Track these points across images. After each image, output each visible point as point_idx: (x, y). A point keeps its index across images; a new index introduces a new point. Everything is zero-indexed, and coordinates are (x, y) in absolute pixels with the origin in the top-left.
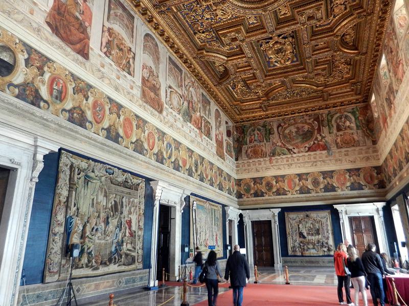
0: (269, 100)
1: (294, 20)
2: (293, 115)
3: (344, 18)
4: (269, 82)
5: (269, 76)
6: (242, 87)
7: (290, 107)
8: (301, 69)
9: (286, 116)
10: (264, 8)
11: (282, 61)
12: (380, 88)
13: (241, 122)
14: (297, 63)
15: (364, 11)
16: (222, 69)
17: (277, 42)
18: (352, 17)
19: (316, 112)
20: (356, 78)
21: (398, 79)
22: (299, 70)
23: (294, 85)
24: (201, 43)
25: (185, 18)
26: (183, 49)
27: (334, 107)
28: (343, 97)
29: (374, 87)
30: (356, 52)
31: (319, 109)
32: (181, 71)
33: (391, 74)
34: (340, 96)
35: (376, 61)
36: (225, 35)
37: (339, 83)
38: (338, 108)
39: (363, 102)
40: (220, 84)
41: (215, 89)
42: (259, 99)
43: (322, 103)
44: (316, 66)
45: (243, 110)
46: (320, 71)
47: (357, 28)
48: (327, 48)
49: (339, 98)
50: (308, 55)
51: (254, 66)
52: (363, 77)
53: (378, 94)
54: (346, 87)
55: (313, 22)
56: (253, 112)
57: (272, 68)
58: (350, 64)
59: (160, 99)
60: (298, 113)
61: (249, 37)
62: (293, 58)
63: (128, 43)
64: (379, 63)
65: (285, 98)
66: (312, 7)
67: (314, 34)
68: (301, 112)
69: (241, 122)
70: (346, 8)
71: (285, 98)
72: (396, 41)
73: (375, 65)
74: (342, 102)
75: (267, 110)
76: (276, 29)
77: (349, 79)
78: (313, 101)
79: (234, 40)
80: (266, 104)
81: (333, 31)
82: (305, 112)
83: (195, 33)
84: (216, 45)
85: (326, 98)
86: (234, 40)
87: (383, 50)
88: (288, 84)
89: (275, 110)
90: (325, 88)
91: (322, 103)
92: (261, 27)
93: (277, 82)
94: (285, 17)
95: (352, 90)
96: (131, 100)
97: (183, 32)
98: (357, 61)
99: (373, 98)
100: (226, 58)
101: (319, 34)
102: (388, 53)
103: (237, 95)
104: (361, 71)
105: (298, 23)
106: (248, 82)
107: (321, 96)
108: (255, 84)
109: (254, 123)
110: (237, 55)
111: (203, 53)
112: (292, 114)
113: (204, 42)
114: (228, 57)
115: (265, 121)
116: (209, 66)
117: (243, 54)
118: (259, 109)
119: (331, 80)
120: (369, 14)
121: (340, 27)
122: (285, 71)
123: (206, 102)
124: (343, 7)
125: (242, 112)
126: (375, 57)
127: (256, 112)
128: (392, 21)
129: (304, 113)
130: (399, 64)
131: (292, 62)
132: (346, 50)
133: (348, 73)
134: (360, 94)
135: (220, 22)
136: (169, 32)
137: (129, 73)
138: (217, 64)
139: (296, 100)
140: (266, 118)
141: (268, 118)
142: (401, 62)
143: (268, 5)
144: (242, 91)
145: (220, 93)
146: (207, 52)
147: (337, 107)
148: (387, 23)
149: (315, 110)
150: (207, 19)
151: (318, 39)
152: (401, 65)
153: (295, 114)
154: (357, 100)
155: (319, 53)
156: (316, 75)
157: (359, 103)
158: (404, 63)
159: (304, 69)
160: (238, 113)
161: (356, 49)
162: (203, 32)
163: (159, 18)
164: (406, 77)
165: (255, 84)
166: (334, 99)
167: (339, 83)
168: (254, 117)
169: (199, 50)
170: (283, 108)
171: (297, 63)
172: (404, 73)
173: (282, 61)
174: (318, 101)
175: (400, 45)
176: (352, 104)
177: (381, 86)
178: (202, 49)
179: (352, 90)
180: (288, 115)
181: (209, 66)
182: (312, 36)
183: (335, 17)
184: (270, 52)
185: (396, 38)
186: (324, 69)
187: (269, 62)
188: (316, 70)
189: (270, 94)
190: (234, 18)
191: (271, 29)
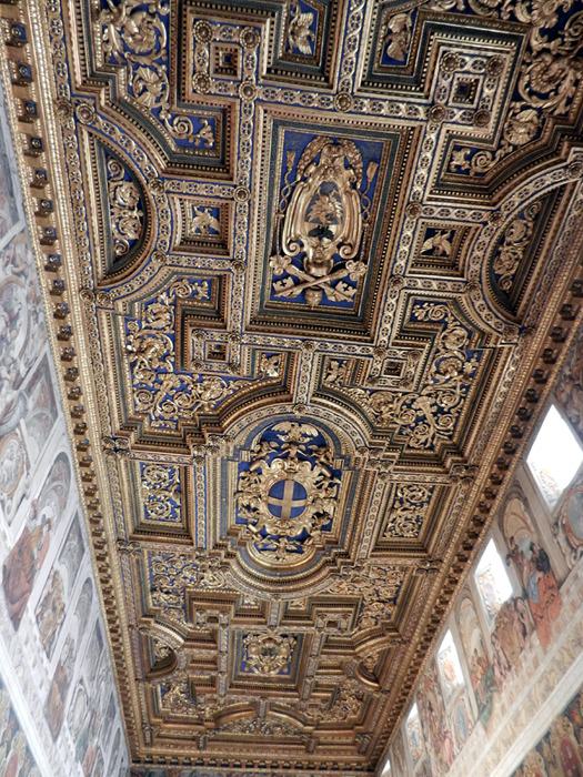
0: (218, 729)
1: (309, 619)
2: (249, 770)
3: (373, 635)
4: (233, 697)
5: (237, 686)
6: (182, 693)
7: (248, 751)
8: (291, 690)
9: (236, 769)
10: (276, 594)
11: (266, 668)
12: (404, 758)
13: (146, 762)
14: (287, 676)
15: (400, 636)
16: (164, 653)
17: (270, 639)
18: (384, 639)
19: (290, 771)
20: (365, 725)
21: (441, 761)
22: (287, 690)
23: (270, 712)
24: (154, 605)
25: (150, 565)
26: (121, 611)
27: (321, 769)
28: (338, 751)
29: (391, 751)
30: (376, 685)
31: (297, 768)
32: (101, 645)
33: (428, 745)
34: (334, 750)
35: (401, 709)
36: (201, 610)
37: (338, 727)
38: (328, 772)
39: (369, 770)
40: (147, 679)
41: (132, 686)
42: (200, 721)
43: (302, 756)
44: (314, 691)
45: (159, 736)
46: (318, 702)
47: (385, 655)
48: (338, 668)
49: (330, 751)
50: (310, 672)
51: (223, 666)
52: (377, 725)
53: (398, 765)
54: (347, 736)
55: (333, 630)
56: (176, 746)
57: (245, 674)
58: (361, 700)
59: (63, 709)
60: (260, 767)
61: (236, 622)
62: (284, 666)
63: (65, 599)
64: (406, 714)
65: (243, 731)
66: (337, 612)
67: (328, 644)
68: (265, 767)
69: (146, 762)
70: (376, 624)
71: (243, 731)
72: (439, 698)
73: (398, 714)
74: (335, 763)
75: (204, 748)
76: (281, 624)
77: (352, 726)
78: (290, 750)
79: (214, 619)
80: (211, 735)
81: (353, 648)
82: (272, 767)
83: (153, 590)
84: (174, 616)
85: (311, 749)
86: (214, 619)
87: (415, 697)
88: (262, 710)
89: (219, 750)
90: (317, 729)
91: (302, 756)
92: (261, 613)
93: (244, 700)
94: (298, 611)
95: (354, 744)
96: (32, 713)
97: (137, 584)
98: (372, 700)
99: (387, 767)
100: (182, 641)
101: (333, 647)
102: (424, 707)
103: (164, 704)
104: (377, 714)
105: (313, 625)
106: (198, 688)
107: (306, 743)
108: (208, 696)
109: (170, 771)
110: (204, 641)
111: (149, 622)
112: (247, 766)
113: (160, 606)
114: (186, 640)
115: (195, 771)
116: (145, 643)
117: (215, 642)
118: (189, 742)
119: (328, 719)
120: (405, 643)
121: (364, 646)
122: (265, 686)
123: (111, 713)
124: (373, 621)
125: (155, 740)
126: (401, 701)
127: (183, 747)
128: (434, 664)
129: (269, 770)
130: (445, 737)
131: (281, 672)
132: (363, 679)
133: (355, 713)
134: (364, 753)
135: (202, 587)
136: (117, 581)
137: (48, 656)
138: (159, 645)
139: (261, 738)
140: (197, 764)
141: (202, 764)
142: (449, 735)
143: (283, 591)
144: (177, 698)
145: (138, 694)
146: (157, 622)
147: (325, 769)
148: (426, 663)
149: (289, 768)
150: (185, 578)
151: (332, 653)
152: (447, 740)
153: (252, 767)
154: (359, 763)
155: (326, 674)
156: (311, 706)
157: (362, 770)
158: (454, 740)
159: (296, 690)
160: (148, 740)
161: (376, 681)
162: (167, 593)
163: (114, 558)
164: (457, 765)
165: (208, 696)
166: (324, 752)
167: (338, 727)
168: (175, 757)
169: (145, 616)
170: (234, 750)
171: (287, 676)
172: (454, 757)
173: (266, 668)
174: (297, 749)
175: (448, 708)
176: (350, 769)
177: (407, 755)
178: (152, 616)
179: (354, 744)
180: (240, 766)
181: (145, 643)
182: (325, 647)
183: (360, 629)
184: (254, 649)
185: (440, 693)
186: (324, 700)
187: (244, 664)
188: (315, 697)
189: (224, 720)
190: (226, 589)
191: (273, 622)
